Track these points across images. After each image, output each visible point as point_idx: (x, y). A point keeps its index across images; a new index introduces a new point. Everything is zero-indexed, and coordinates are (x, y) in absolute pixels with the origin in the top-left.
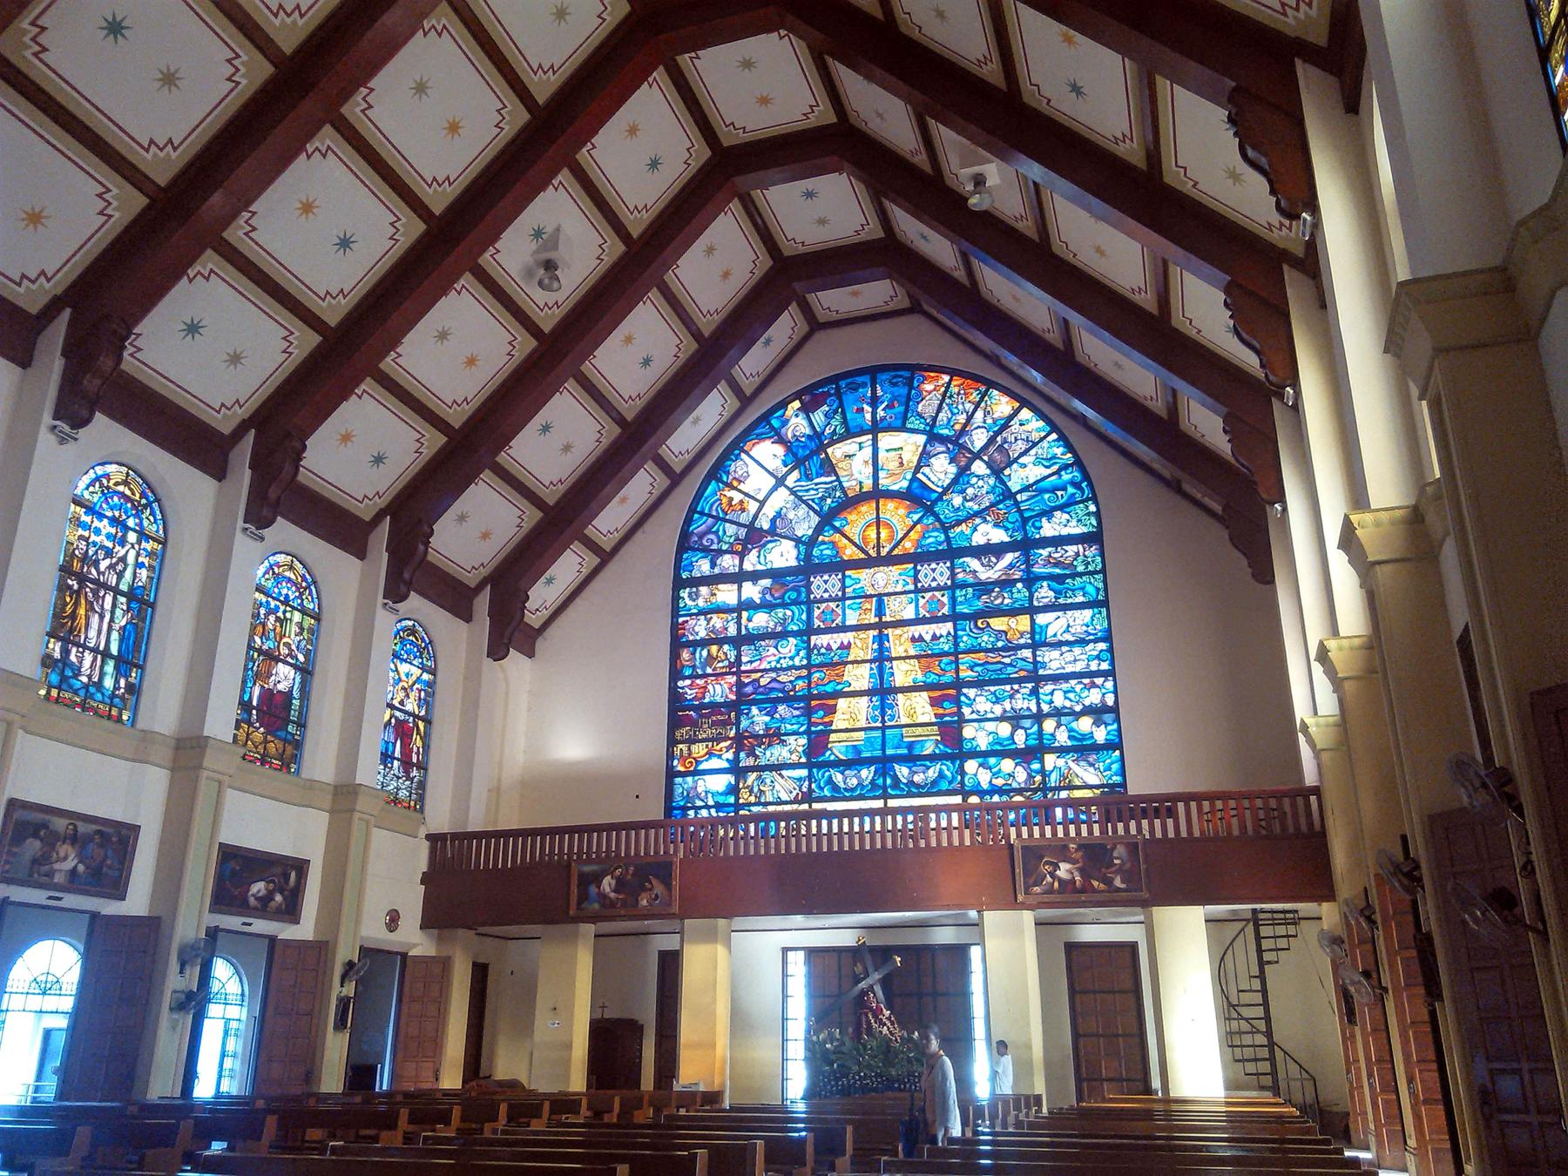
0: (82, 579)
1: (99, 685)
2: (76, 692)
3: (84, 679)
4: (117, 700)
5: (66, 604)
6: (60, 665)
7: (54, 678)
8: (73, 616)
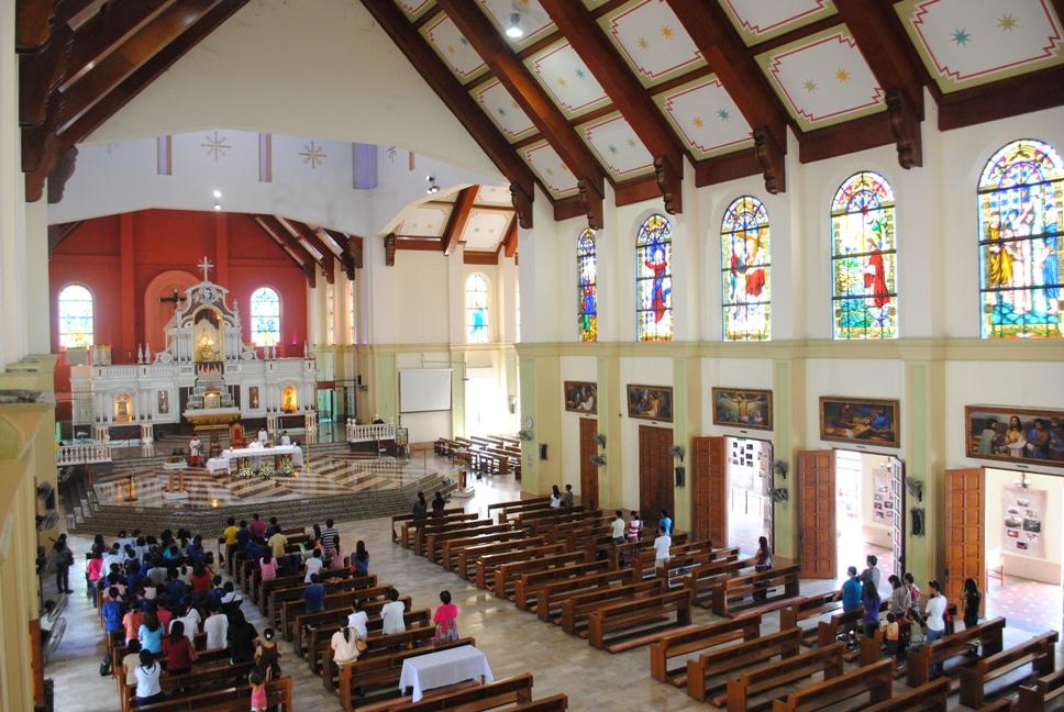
0: (1001, 242)
1: (1032, 312)
2: (1014, 322)
3: (1019, 311)
4: (1050, 319)
5: (992, 265)
6: (998, 308)
7: (996, 318)
8: (1000, 270)
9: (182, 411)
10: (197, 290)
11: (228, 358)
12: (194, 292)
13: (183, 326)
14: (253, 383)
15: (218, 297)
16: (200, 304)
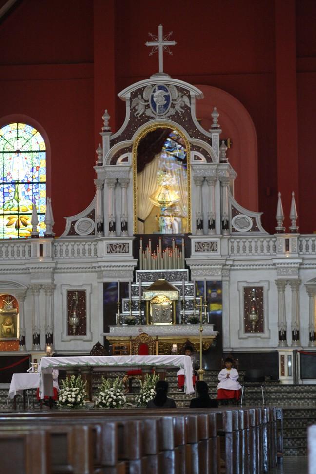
9: (106, 330)
10: (140, 91)
11: (200, 226)
12: (134, 95)
13: (113, 162)
14: (254, 278)
15: (180, 102)
16: (146, 119)
